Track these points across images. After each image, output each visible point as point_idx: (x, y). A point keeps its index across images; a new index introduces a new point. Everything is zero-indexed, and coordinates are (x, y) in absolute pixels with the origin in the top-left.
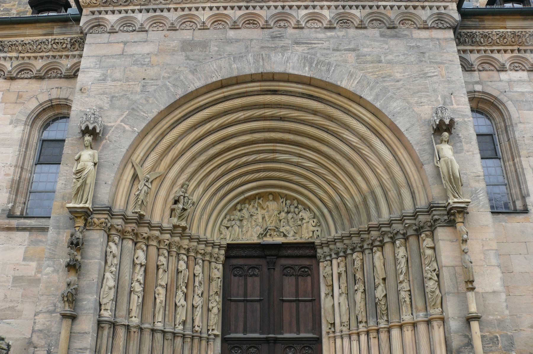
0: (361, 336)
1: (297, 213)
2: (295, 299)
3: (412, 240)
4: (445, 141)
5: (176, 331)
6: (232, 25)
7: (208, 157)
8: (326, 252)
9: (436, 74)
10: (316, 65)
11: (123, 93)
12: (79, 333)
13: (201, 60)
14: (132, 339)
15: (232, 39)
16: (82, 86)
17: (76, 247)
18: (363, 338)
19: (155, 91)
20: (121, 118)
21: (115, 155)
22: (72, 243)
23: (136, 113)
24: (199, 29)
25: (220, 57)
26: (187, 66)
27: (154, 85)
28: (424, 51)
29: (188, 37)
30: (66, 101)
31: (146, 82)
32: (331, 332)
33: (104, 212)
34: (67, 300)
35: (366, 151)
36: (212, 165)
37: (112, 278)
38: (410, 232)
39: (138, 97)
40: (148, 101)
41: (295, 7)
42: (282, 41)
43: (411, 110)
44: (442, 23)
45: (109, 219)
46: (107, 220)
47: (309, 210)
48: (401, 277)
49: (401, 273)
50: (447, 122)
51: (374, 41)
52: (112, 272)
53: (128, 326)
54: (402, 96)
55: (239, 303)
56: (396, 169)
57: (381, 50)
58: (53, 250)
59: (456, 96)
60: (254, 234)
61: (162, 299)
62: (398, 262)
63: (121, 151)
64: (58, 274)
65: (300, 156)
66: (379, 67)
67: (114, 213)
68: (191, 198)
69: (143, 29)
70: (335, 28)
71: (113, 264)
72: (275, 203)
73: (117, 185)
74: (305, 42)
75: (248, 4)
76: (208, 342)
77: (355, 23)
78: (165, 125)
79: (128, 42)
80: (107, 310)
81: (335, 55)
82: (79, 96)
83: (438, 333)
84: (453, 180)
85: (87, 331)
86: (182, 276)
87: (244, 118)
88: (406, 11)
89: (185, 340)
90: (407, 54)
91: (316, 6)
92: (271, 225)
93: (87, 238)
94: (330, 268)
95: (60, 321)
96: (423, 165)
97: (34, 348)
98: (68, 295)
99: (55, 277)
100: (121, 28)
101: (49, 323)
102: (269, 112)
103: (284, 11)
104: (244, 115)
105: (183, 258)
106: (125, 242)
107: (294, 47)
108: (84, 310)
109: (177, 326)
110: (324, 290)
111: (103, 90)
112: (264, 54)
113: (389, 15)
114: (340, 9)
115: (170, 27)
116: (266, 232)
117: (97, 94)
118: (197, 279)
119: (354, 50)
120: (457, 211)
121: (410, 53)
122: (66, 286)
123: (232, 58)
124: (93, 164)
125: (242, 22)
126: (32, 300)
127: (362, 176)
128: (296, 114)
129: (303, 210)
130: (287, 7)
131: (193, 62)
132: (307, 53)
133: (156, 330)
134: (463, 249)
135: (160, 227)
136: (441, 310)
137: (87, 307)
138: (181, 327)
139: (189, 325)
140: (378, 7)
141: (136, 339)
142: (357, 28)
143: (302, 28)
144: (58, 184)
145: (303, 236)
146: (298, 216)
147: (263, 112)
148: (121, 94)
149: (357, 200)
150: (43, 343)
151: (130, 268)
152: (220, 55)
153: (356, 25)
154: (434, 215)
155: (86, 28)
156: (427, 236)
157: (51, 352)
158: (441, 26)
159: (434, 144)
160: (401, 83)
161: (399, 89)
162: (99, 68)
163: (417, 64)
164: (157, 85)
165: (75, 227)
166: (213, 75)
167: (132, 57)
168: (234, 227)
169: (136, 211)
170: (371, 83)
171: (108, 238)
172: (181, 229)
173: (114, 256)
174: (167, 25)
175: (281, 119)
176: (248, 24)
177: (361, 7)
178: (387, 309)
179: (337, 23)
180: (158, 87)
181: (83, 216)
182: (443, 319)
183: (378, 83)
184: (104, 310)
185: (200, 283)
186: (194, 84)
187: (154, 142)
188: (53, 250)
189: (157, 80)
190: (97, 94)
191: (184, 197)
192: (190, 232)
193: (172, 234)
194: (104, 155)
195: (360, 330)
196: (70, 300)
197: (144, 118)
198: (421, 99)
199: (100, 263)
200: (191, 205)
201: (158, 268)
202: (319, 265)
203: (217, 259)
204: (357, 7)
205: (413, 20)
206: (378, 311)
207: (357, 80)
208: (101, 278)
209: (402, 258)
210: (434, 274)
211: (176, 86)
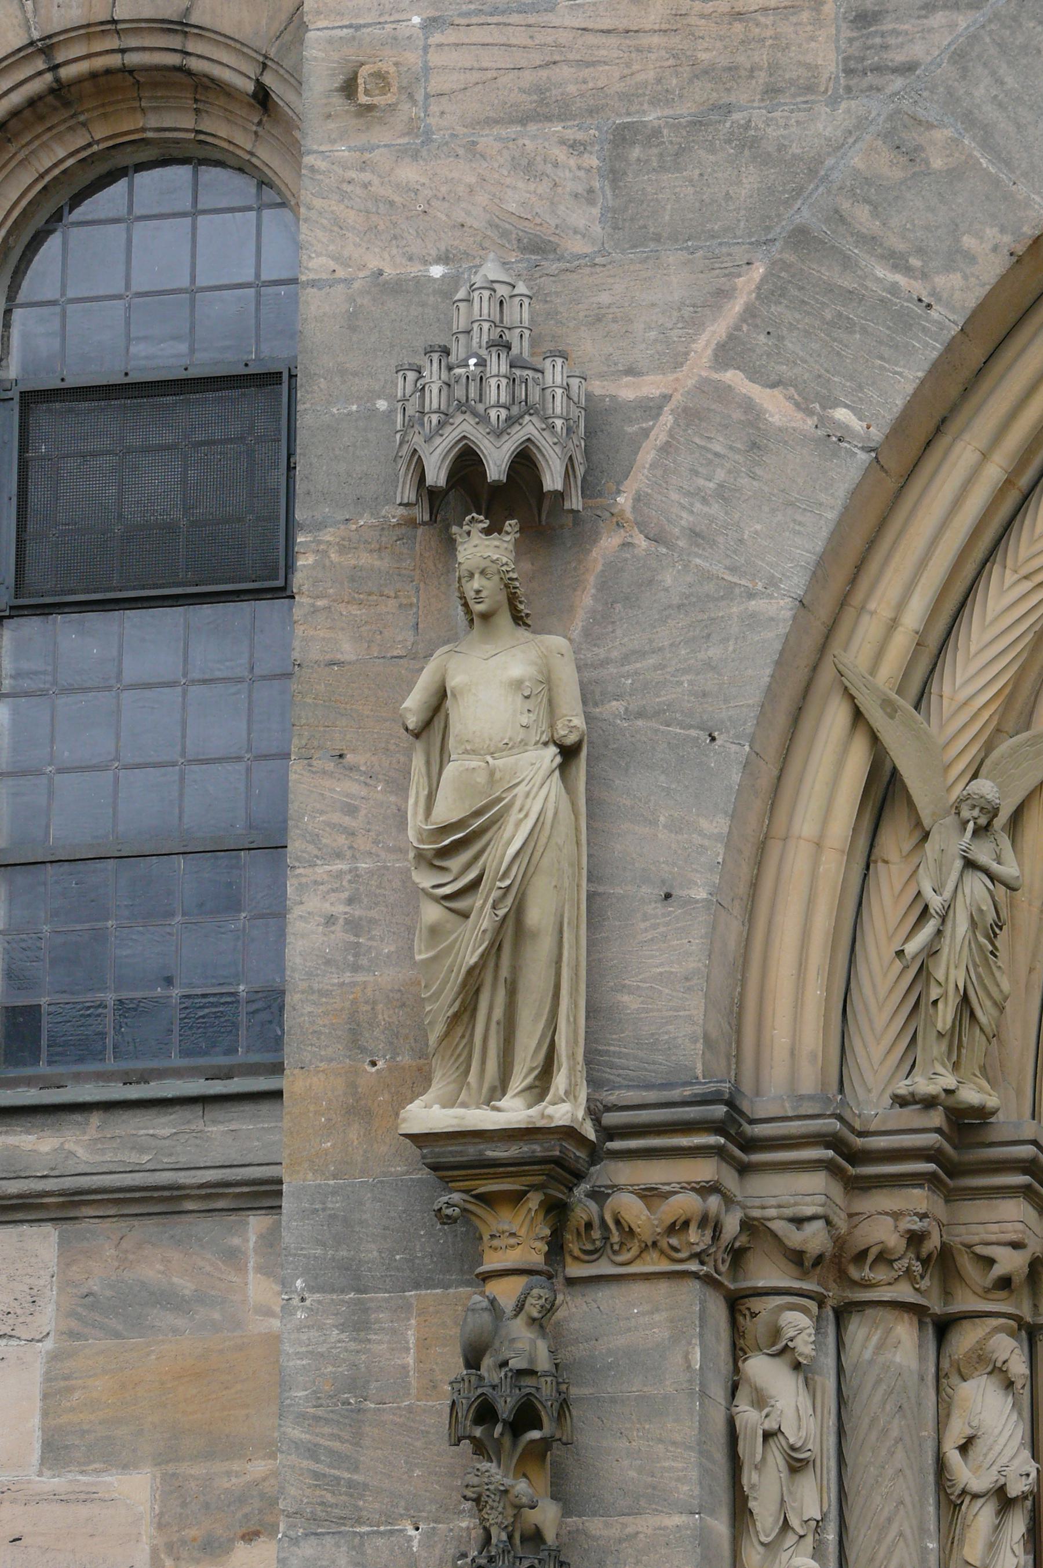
11: (702, 93)
19: (959, 57)
20: (718, 329)
21: (714, 652)
22: (485, 1413)
30: (175, 42)
33: (684, 1141)
45: (730, 1180)
46: (714, 1202)
58: (338, 1459)
63: (752, 620)
71: (794, 1522)
73: (754, 885)
82: (342, 150)
93: (578, 1351)
111: (528, 77)
124: (550, 756)
148: (685, 109)
151: (922, 1530)
165: (487, 1277)
171: (734, 1324)
173: (796, 1466)
188: (338, 1459)
194: (625, 659)
199: (703, 1537)
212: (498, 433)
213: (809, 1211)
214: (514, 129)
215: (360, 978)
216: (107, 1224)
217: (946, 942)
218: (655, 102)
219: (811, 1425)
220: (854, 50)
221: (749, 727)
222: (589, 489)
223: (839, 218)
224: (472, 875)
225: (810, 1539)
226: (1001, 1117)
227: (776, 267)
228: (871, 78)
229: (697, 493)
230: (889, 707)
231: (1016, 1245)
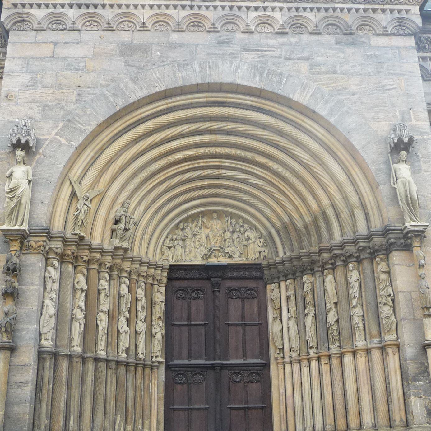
0: (312, 362)
1: (242, 232)
2: (241, 323)
3: (366, 264)
4: (403, 161)
5: (119, 359)
6: (176, 28)
7: (151, 173)
8: (273, 274)
9: (394, 86)
10: (266, 75)
11: (57, 101)
12: (18, 365)
15: (177, 43)
16: (8, 92)
17: (13, 273)
18: (314, 364)
19: (92, 100)
20: (56, 131)
21: (52, 171)
22: (8, 269)
24: (139, 31)
25: (163, 64)
27: (92, 94)
29: (127, 39)
32: (280, 358)
33: (41, 235)
35: (317, 169)
36: (154, 181)
37: (53, 305)
39: (73, 107)
40: (85, 112)
41: (244, 8)
42: (230, 47)
44: (403, 29)
45: (47, 241)
46: (45, 243)
47: (255, 229)
48: (355, 302)
49: (354, 297)
50: (406, 140)
51: (329, 49)
52: (52, 299)
53: (70, 355)
55: (183, 328)
56: (349, 189)
57: (336, 60)
60: (198, 255)
61: (104, 326)
62: (351, 286)
63: (58, 168)
65: (247, 172)
67: (52, 235)
68: (133, 217)
69: (75, 28)
70: (287, 33)
72: (220, 221)
73: (54, 204)
74: (255, 48)
75: (193, 3)
76: (152, 370)
77: (309, 28)
78: (104, 138)
79: (59, 43)
81: (287, 64)
82: (5, 104)
83: (393, 361)
84: (410, 202)
85: (27, 363)
86: (125, 301)
87: (189, 131)
88: (365, 15)
90: (364, 64)
91: (267, 7)
92: (216, 245)
93: (23, 263)
94: (278, 290)
96: (379, 185)
100: (50, 26)
102: (215, 125)
103: (233, 12)
104: (189, 128)
105: (124, 282)
107: (242, 54)
108: (24, 340)
109: (120, 354)
110: (271, 314)
111: (33, 98)
112: (210, 61)
113: (346, 19)
114: (293, 12)
115: (106, 27)
116: (210, 253)
117: (26, 102)
118: (139, 304)
119: (307, 59)
120: (415, 235)
123: (176, 65)
124: (27, 181)
125: (186, 25)
127: (313, 195)
128: (244, 129)
129: (249, 230)
130: (235, 8)
131: (133, 69)
132: (257, 62)
134: (420, 274)
135: (101, 249)
136: (396, 336)
137: (27, 337)
138: (124, 355)
140: (334, 10)
141: (79, 369)
142: (311, 33)
143: (252, 32)
145: (249, 257)
146: (243, 235)
147: (209, 125)
148: (54, 103)
149: (307, 220)
152: (163, 61)
153: (310, 30)
154: (390, 238)
155: (8, 24)
156: (382, 260)
158: (402, 32)
159: (391, 164)
160: (357, 96)
161: (355, 103)
162: (27, 72)
163: (375, 75)
164: (95, 94)
166: (156, 84)
167: (63, 60)
168: (176, 247)
169: (76, 232)
170: (325, 96)
171: (46, 262)
172: (123, 251)
174: (102, 25)
175: (228, 133)
176: (193, 26)
177: (315, 10)
178: (339, 334)
179: (289, 28)
181: (18, 239)
182: (398, 346)
183: (332, 96)
184: (45, 339)
185: (143, 307)
186: (135, 94)
187: (93, 157)
189: (94, 88)
190: (26, 102)
193: (113, 256)
197: (82, 131)
200: (133, 225)
202: (266, 287)
203: (159, 282)
204: (312, 9)
205: (372, 25)
206: (330, 336)
207: (311, 93)
210: (389, 299)
211: (115, 95)
213: (58, 247)
217: (81, 214)
219: (56, 277)
220: (78, 98)
221: (56, 181)
226: (86, 238)
230: (75, 182)
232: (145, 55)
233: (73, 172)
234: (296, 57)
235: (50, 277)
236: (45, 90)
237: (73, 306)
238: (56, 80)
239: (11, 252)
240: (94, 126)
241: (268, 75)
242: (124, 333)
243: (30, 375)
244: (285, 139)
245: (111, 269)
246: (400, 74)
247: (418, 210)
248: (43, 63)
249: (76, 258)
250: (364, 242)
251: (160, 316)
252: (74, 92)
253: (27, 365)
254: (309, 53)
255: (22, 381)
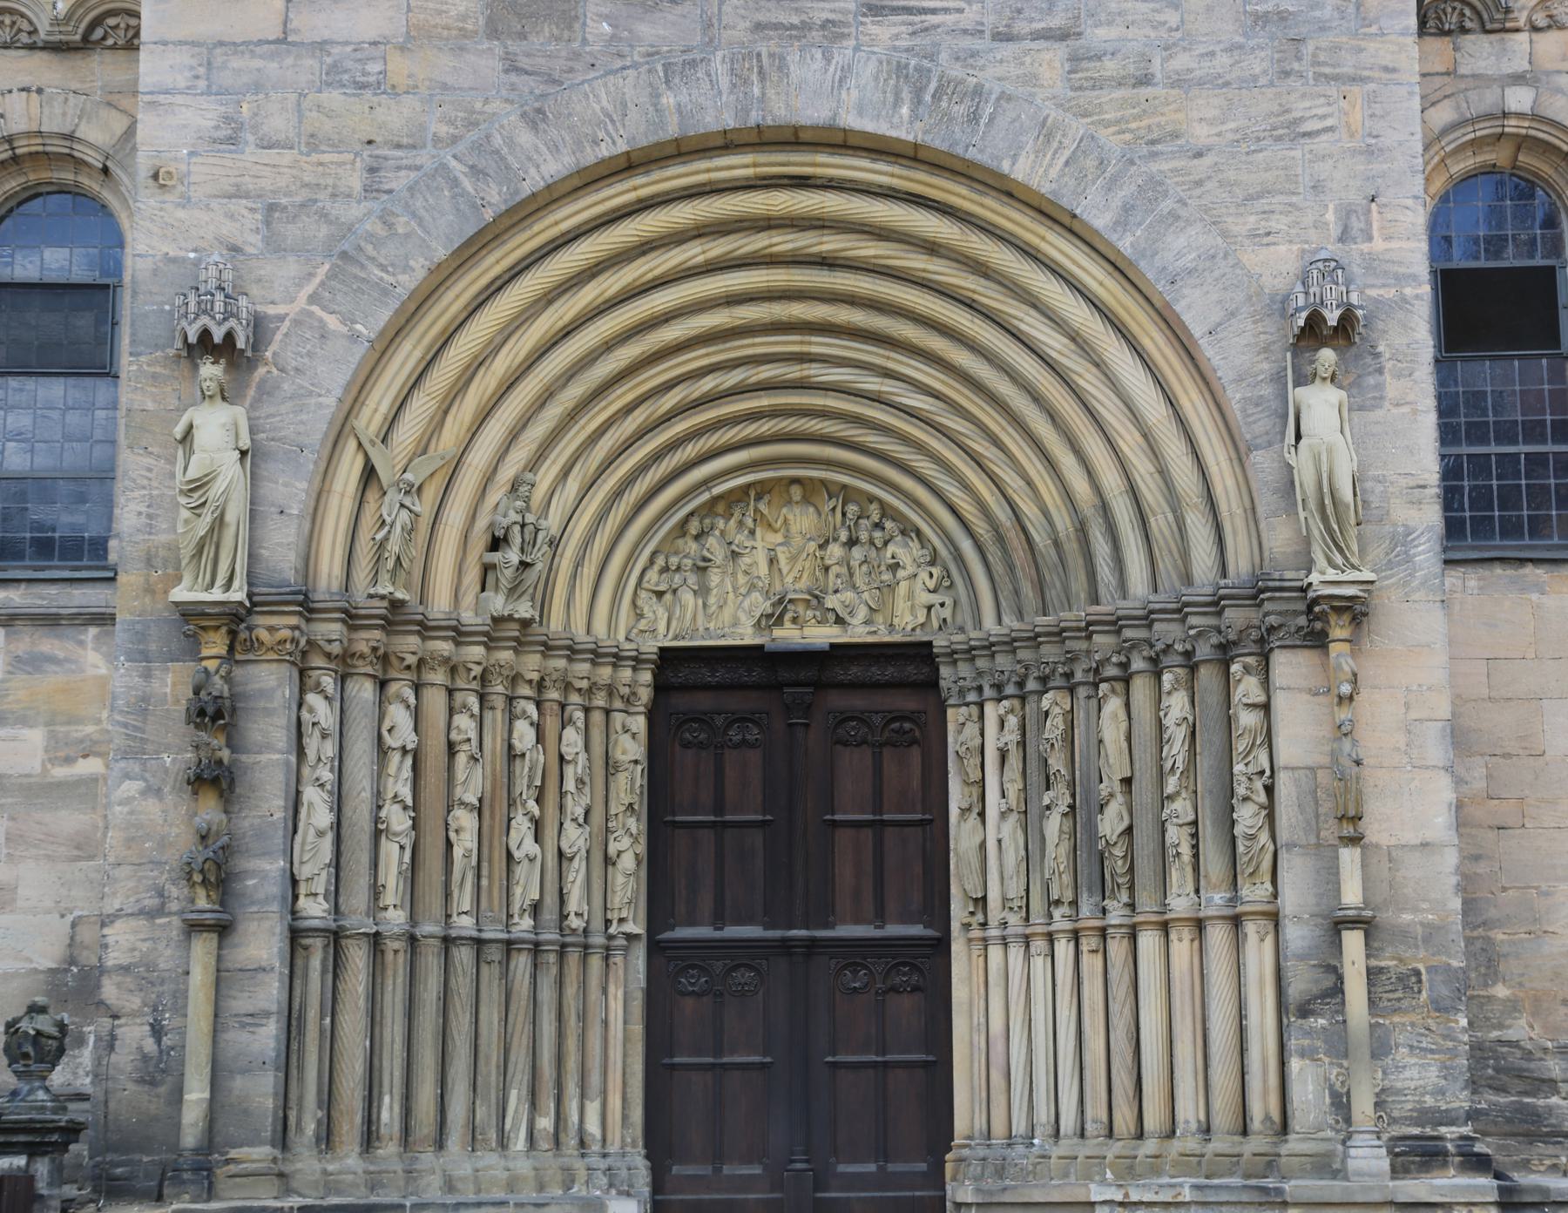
5: (513, 936)
9: (1329, 122)
10: (933, 96)
12: (240, 970)
13: (556, 76)
14: (389, 972)
16: (158, 163)
19: (411, 189)
20: (309, 289)
21: (304, 417)
22: (202, 713)
23: (356, 271)
25: (619, 63)
26: (511, 97)
27: (409, 168)
28: (1304, 30)
31: (377, 157)
33: (286, 609)
34: (203, 881)
38: (1204, 651)
39: (355, 211)
43: (1231, 261)
45: (303, 625)
46: (297, 633)
48: (1172, 784)
52: (322, 786)
53: (377, 934)
54: (1206, 212)
57: (1153, 34)
58: (136, 728)
59: (1385, 205)
61: (469, 845)
63: (320, 406)
64: (161, 799)
66: (1143, 100)
68: (543, 523)
71: (323, 758)
73: (316, 509)
78: (451, 304)
80: (316, 895)
81: (999, 57)
82: (152, 202)
85: (264, 964)
86: (526, 769)
89: (539, 960)
90: (1241, 47)
93: (239, 689)
95: (182, 938)
97: (110, 1020)
98: (206, 866)
99: (152, 807)
101: (148, 944)
105: (524, 712)
106: (353, 686)
107: (862, 23)
108: (253, 903)
109: (516, 919)
111: (233, 180)
119: (1063, 36)
121: (1251, 43)
122: (194, 839)
123: (660, 68)
124: (237, 454)
126: (42, 852)
131: (530, 81)
132: (907, 50)
133: (455, 938)
135: (454, 629)
137: (261, 895)
138: (527, 923)
139: (549, 914)
141: (401, 971)
144: (126, 515)
148: (298, 199)
150: (135, 1002)
152: (620, 56)
157: (162, 1027)
160: (1208, 160)
161: (1199, 183)
162: (208, 92)
163: (1271, 84)
164: (418, 168)
166: (601, 135)
167: (318, 53)
169: (382, 591)
171: (301, 680)
172: (516, 626)
173: (324, 736)
180: (420, 174)
183: (1132, 162)
184: (307, 895)
186: (538, 167)
189: (414, 147)
191: (523, 526)
192: (543, 630)
193: (491, 641)
194: (267, 417)
195: (1053, 928)
196: (212, 879)
198: (1267, 220)
199: (287, 763)
200: (545, 548)
201: (452, 750)
206: (1108, 876)
207: (1067, 153)
208: (291, 804)
209: (1178, 725)
212: (219, 324)
214: (225, 201)
215: (152, 537)
216: (25, 628)
218: (285, 195)
219: (331, 720)
220: (367, 182)
221: (317, 447)
222: (255, 348)
223: (359, 248)
224: (203, 500)
225: (329, 765)
227: (334, 266)
228: (374, 194)
229: (298, 354)
230: (373, 443)
231: (413, 653)
232: (566, 34)
233: (366, 412)
234: (1027, 30)
235: (314, 724)
236: (271, 156)
237: (378, 794)
238: (300, 122)
239: (205, 663)
240: (421, 274)
241: (937, 96)
242: (526, 862)
243: (271, 992)
244: (993, 285)
245: (484, 678)
246: (1354, 80)
247: (1353, 532)
248: (257, 63)
249: (385, 660)
250: (1205, 614)
251: (631, 804)
252: (353, 163)
253: (264, 970)
254: (1070, 15)
255: (251, 1010)
